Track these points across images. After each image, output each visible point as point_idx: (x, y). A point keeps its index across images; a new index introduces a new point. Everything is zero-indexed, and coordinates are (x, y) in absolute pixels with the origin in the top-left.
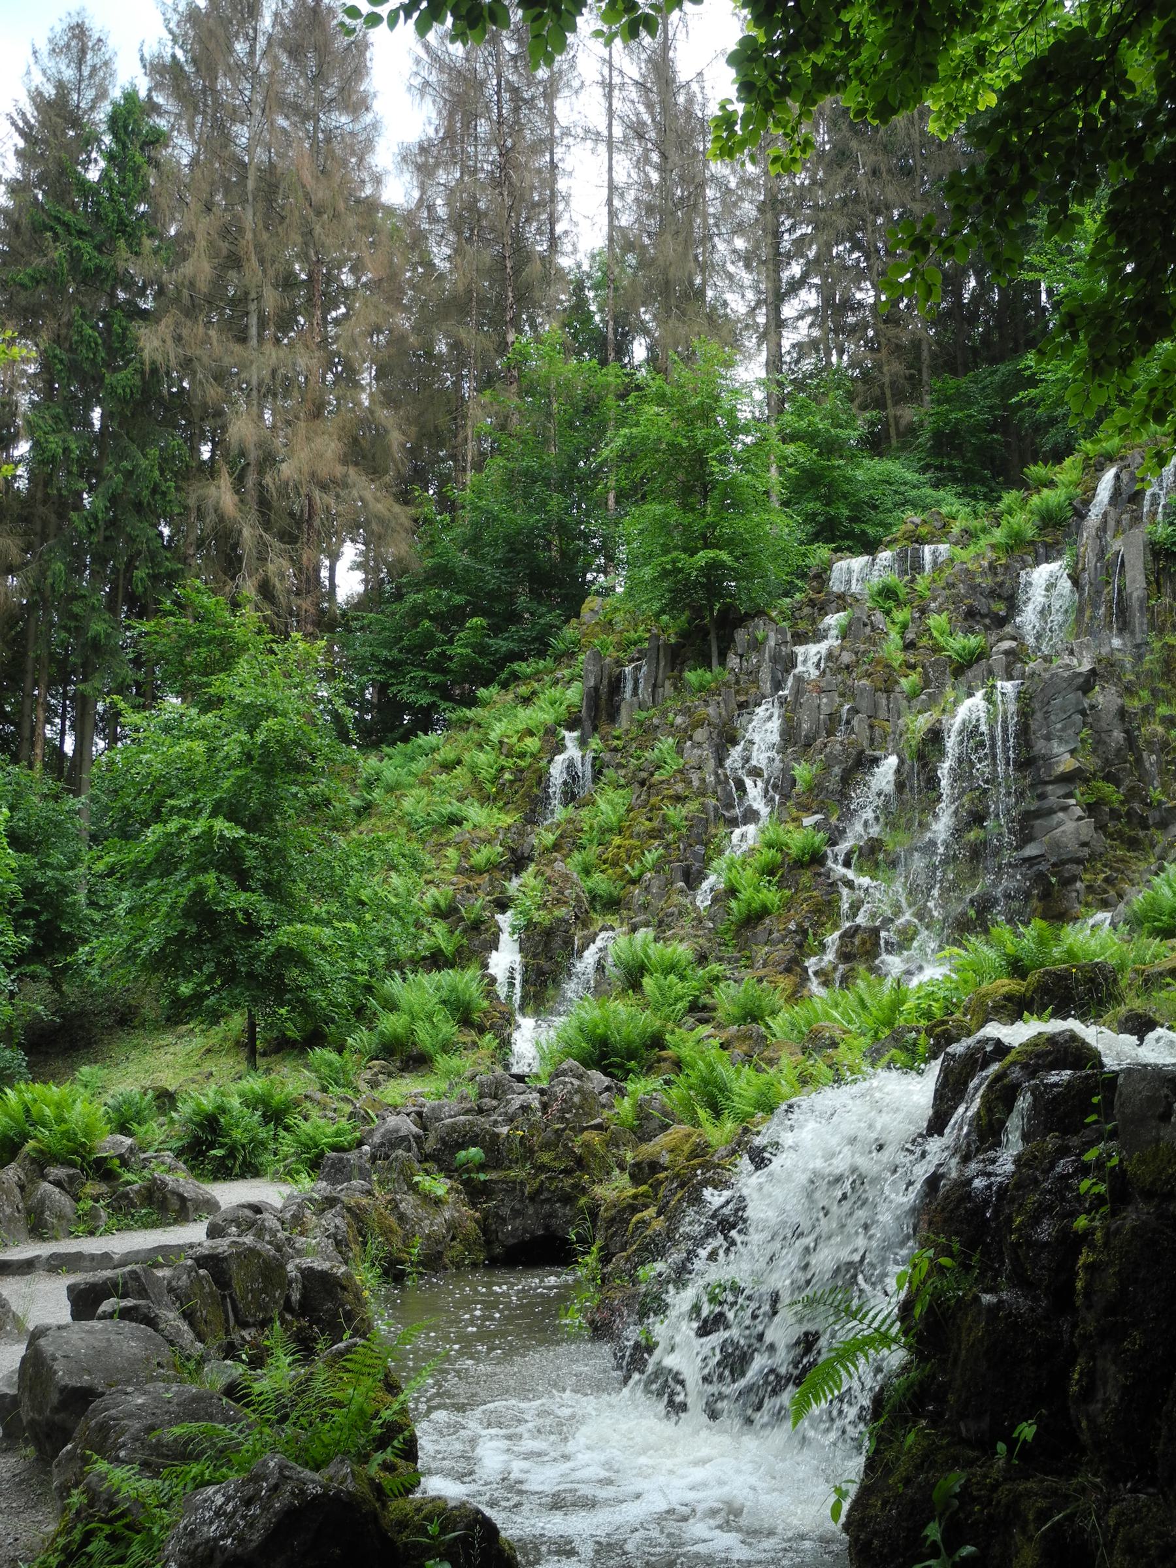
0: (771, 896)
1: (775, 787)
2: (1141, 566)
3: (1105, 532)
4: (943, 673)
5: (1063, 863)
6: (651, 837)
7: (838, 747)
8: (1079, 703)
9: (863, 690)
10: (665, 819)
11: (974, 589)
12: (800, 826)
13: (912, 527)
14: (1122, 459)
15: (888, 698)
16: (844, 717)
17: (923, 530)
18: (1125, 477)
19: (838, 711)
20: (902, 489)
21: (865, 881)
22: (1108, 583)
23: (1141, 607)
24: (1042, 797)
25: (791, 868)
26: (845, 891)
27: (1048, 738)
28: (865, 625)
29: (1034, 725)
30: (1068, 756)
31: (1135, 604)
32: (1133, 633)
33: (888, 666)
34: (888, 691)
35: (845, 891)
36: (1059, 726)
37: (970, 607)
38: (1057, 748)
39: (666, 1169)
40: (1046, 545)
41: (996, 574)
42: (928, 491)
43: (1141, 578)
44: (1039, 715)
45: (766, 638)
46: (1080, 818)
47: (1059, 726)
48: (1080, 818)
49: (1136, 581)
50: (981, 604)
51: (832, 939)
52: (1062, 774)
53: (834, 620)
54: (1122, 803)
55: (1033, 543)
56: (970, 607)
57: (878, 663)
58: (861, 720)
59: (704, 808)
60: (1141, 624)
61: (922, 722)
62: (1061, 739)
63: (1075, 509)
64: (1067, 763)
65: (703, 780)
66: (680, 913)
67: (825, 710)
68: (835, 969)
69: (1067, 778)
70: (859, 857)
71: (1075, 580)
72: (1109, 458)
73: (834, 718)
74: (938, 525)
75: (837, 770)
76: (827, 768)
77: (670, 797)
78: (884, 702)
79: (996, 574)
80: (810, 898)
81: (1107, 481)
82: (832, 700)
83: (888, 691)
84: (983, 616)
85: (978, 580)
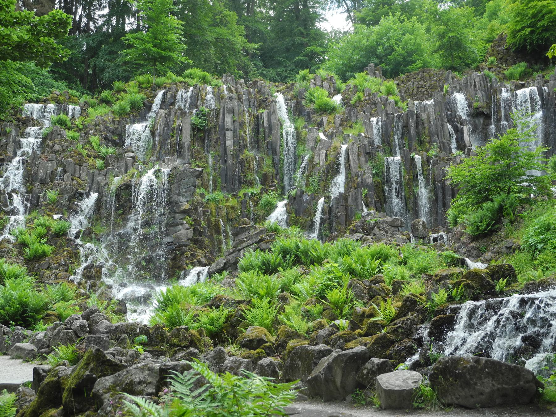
0: (48, 248)
1: (27, 200)
2: (189, 132)
3: (170, 115)
4: (114, 161)
5: (181, 246)
7: (68, 186)
8: (194, 182)
9: (69, 163)
11: (106, 128)
12: (53, 217)
13: (56, 96)
14: (165, 88)
15: (80, 168)
17: (61, 98)
18: (169, 95)
19: (56, 170)
20: (41, 77)
21: (88, 245)
22: (173, 137)
24: (174, 218)
25: (52, 237)
26: (81, 249)
27: (179, 195)
28: (58, 135)
29: (173, 189)
30: (186, 203)
31: (186, 147)
32: (184, 159)
33: (80, 154)
34: (80, 165)
35: (81, 249)
36: (184, 190)
37: (106, 135)
38: (182, 199)
39: (267, 342)
40: (133, 116)
41: (114, 124)
42: (53, 81)
43: (189, 137)
44: (176, 185)
45: (11, 131)
46: (188, 229)
47: (184, 190)
48: (188, 229)
50: (109, 135)
51: (80, 270)
52: (184, 210)
53: (32, 130)
54: (192, 225)
55: (128, 114)
56: (106, 135)
57: (75, 152)
58: (68, 176)
60: (188, 155)
61: (117, 181)
62: (184, 196)
63: (144, 103)
64: (186, 206)
66: (8, 251)
67: (50, 169)
68: (86, 282)
69: (184, 212)
70: (84, 234)
71: (153, 133)
72: (159, 86)
73: (53, 173)
74: (68, 97)
75: (66, 196)
76: (61, 193)
78: (78, 169)
79: (114, 124)
80: (67, 250)
81: (160, 94)
82: (53, 165)
83: (80, 165)
84: (109, 140)
85: (108, 125)
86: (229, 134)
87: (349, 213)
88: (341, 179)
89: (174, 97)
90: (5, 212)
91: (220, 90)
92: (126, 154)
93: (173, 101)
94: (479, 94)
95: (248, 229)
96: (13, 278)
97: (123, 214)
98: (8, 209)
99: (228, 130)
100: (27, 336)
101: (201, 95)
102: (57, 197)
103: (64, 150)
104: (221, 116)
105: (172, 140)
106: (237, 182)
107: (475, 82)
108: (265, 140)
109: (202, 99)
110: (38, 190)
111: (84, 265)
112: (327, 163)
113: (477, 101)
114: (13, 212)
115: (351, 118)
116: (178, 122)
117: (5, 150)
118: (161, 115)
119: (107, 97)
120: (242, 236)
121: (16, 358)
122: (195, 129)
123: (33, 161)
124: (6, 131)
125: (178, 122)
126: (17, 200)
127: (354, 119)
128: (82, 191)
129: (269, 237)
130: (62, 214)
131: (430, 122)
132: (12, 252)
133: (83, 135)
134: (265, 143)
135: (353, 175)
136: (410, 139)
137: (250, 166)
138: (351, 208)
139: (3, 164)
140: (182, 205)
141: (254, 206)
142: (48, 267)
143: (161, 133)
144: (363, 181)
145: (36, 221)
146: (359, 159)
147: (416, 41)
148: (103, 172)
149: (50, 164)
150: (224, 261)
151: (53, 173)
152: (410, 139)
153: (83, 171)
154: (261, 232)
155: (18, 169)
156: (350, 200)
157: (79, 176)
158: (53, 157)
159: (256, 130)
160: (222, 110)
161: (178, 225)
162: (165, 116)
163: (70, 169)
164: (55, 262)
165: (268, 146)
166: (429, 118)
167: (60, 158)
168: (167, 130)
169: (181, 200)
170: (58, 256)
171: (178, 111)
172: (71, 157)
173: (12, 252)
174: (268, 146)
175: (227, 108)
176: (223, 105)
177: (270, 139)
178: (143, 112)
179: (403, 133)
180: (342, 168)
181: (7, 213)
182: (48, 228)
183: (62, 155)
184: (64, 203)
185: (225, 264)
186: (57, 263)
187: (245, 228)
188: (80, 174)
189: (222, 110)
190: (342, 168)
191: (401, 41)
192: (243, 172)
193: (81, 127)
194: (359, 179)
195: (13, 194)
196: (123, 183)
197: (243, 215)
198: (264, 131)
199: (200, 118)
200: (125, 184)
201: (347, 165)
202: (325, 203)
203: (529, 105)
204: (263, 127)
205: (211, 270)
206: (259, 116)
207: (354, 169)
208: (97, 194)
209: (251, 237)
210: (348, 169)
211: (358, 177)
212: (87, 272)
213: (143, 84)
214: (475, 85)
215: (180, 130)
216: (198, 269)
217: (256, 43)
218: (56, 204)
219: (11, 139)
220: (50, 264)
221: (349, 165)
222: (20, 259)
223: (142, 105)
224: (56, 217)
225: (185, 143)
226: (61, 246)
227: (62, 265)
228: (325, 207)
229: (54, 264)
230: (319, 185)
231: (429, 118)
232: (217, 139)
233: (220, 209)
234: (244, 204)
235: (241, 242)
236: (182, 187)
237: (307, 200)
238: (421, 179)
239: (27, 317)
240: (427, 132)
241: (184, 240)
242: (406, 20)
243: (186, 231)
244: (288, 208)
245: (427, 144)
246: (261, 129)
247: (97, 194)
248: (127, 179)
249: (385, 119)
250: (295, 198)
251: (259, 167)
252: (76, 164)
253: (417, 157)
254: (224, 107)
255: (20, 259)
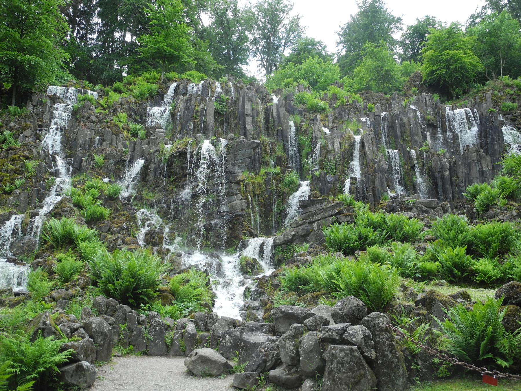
1: (69, 163)
6: (16, 173)
7: (115, 151)
10: (23, 166)
11: (130, 108)
15: (116, 138)
16: (97, 142)
18: (181, 87)
22: (196, 118)
23: (212, 129)
25: (106, 200)
27: (234, 165)
31: (211, 128)
33: (117, 125)
34: (117, 136)
36: (240, 161)
43: (213, 119)
44: (232, 155)
45: (46, 102)
46: (241, 199)
48: (241, 199)
49: (210, 119)
58: (107, 145)
59: (40, 165)
62: (239, 166)
65: (38, 153)
67: (89, 137)
73: (92, 141)
77: (24, 157)
78: (115, 139)
81: (173, 85)
83: (117, 136)
85: (132, 106)
86: (249, 120)
87: (377, 193)
88: (356, 164)
89: (186, 88)
90: (50, 173)
91: (227, 85)
92: (157, 130)
93: (185, 91)
94: (430, 110)
95: (321, 202)
96: (87, 241)
97: (175, 181)
98: (53, 170)
99: (248, 115)
100: (169, 326)
101: (211, 88)
102: (105, 162)
103: (99, 121)
104: (240, 104)
105: (196, 121)
106: (257, 162)
107: (426, 100)
108: (274, 129)
109: (212, 91)
110: (80, 155)
111: (144, 231)
112: (343, 150)
113: (428, 114)
114: (57, 174)
115: (342, 118)
116: (202, 106)
117: (42, 118)
118: (181, 101)
119: (119, 87)
120: (313, 209)
121: (203, 377)
122: (217, 113)
123: (70, 129)
124: (42, 101)
125: (202, 106)
126: (60, 162)
127: (345, 118)
128: (125, 159)
129: (348, 210)
130: (109, 178)
131: (410, 125)
132: (74, 212)
133: (112, 111)
134: (275, 132)
135: (370, 162)
136: (396, 138)
137: (266, 149)
138: (378, 189)
139: (42, 130)
140: (238, 175)
141: (277, 184)
142: (109, 230)
143: (182, 115)
144: (380, 167)
145: (88, 183)
146: (373, 148)
147: (458, 42)
148: (146, 141)
149: (89, 132)
150: (293, 233)
151: (92, 141)
152: (396, 138)
153: (120, 142)
154: (337, 205)
155: (56, 134)
156: (377, 182)
157: (115, 145)
158: (91, 126)
159: (267, 120)
160: (241, 98)
161: (233, 195)
162: (186, 101)
163: (108, 138)
164: (116, 226)
165: (278, 134)
166: (409, 121)
167: (96, 128)
168: (188, 113)
169: (236, 171)
170: (116, 219)
171: (198, 98)
172: (109, 127)
173: (74, 212)
174: (278, 134)
175: (248, 96)
176: (242, 94)
177: (280, 128)
178: (157, 99)
179: (389, 132)
180: (357, 154)
181: (52, 174)
182: (101, 191)
183: (99, 126)
184: (110, 168)
185: (293, 235)
186: (119, 227)
187: (317, 200)
188: (117, 144)
189: (241, 98)
190: (357, 154)
191: (322, 77)
192: (261, 154)
193: (105, 106)
194: (376, 165)
195: (56, 156)
196: (176, 150)
197: (267, 191)
198: (274, 121)
199: (220, 104)
200: (179, 152)
201: (362, 153)
202: (351, 184)
203: (465, 121)
204: (273, 117)
205: (277, 241)
206: (269, 108)
207: (369, 157)
208: (144, 161)
209: (325, 210)
210: (363, 155)
211: (375, 163)
212: (151, 238)
213: (149, 79)
214: (426, 103)
215: (204, 112)
216: (259, 240)
217: (222, 65)
218: (103, 168)
219: (47, 109)
220: (110, 228)
221: (365, 153)
222: (82, 221)
223: (156, 94)
224: (106, 180)
225: (209, 124)
226: (117, 210)
227: (124, 229)
228: (352, 187)
229: (115, 227)
230: (336, 168)
231: (409, 121)
232: (236, 124)
233: (248, 184)
234: (267, 182)
235: (312, 215)
236: (238, 157)
237: (331, 181)
238: (417, 169)
239: (141, 294)
240: (408, 133)
241: (239, 209)
242: (322, 62)
243: (240, 201)
244: (312, 187)
245: (409, 142)
246: (271, 119)
247: (144, 161)
248: (182, 147)
249: (373, 119)
250: (318, 178)
251: (272, 151)
252: (113, 134)
253: (413, 152)
254: (243, 97)
255: (82, 221)
